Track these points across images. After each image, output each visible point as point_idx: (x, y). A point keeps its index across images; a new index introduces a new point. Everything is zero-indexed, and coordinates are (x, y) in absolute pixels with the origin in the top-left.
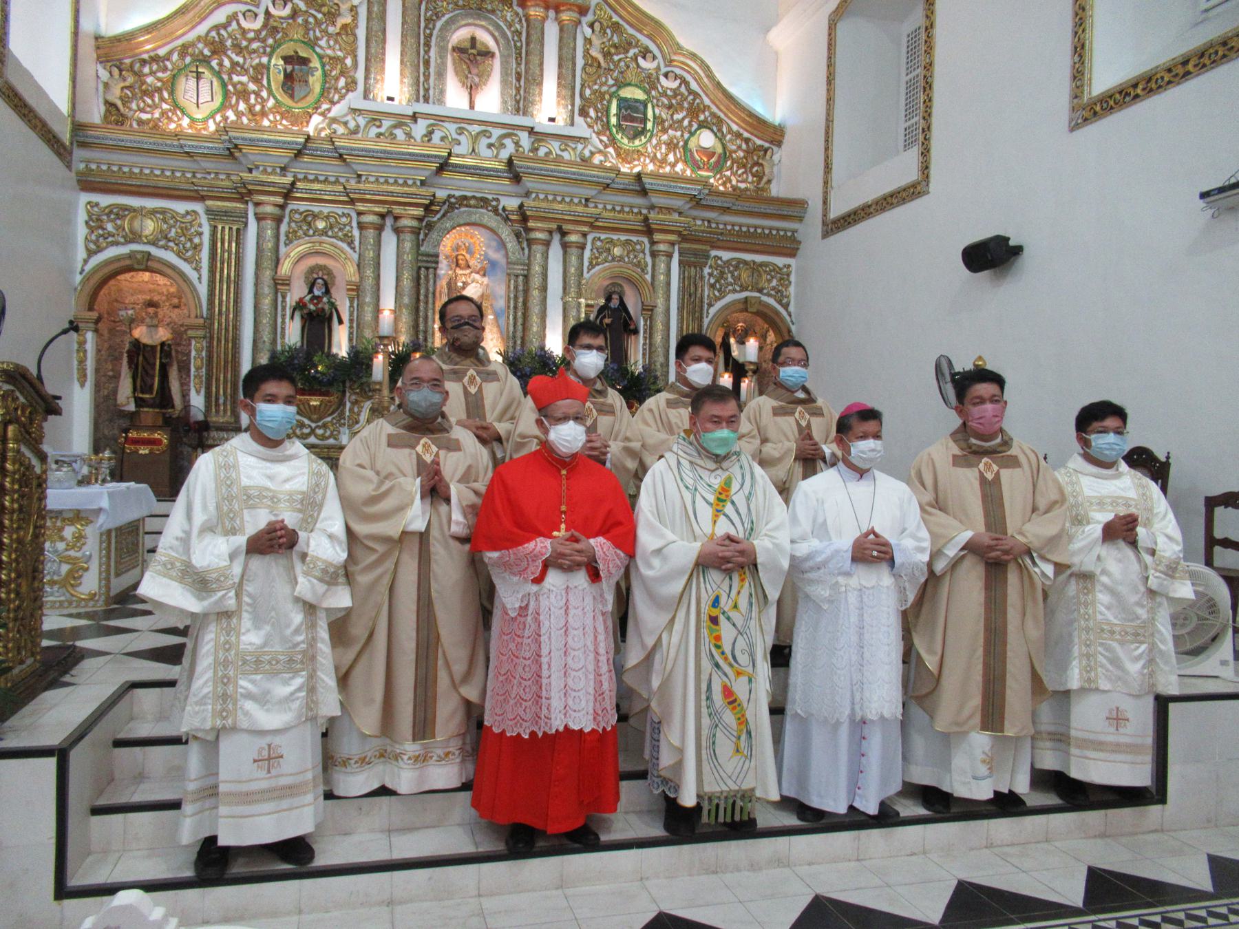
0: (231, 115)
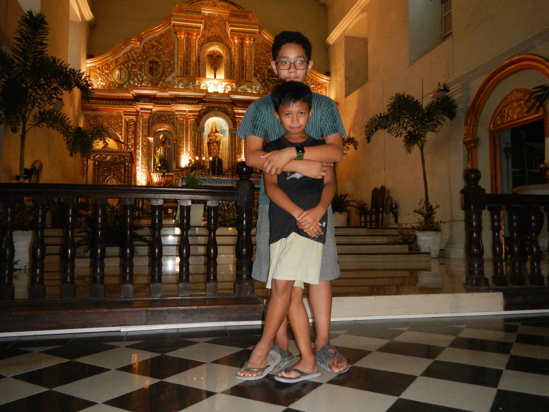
0: (132, 82)
